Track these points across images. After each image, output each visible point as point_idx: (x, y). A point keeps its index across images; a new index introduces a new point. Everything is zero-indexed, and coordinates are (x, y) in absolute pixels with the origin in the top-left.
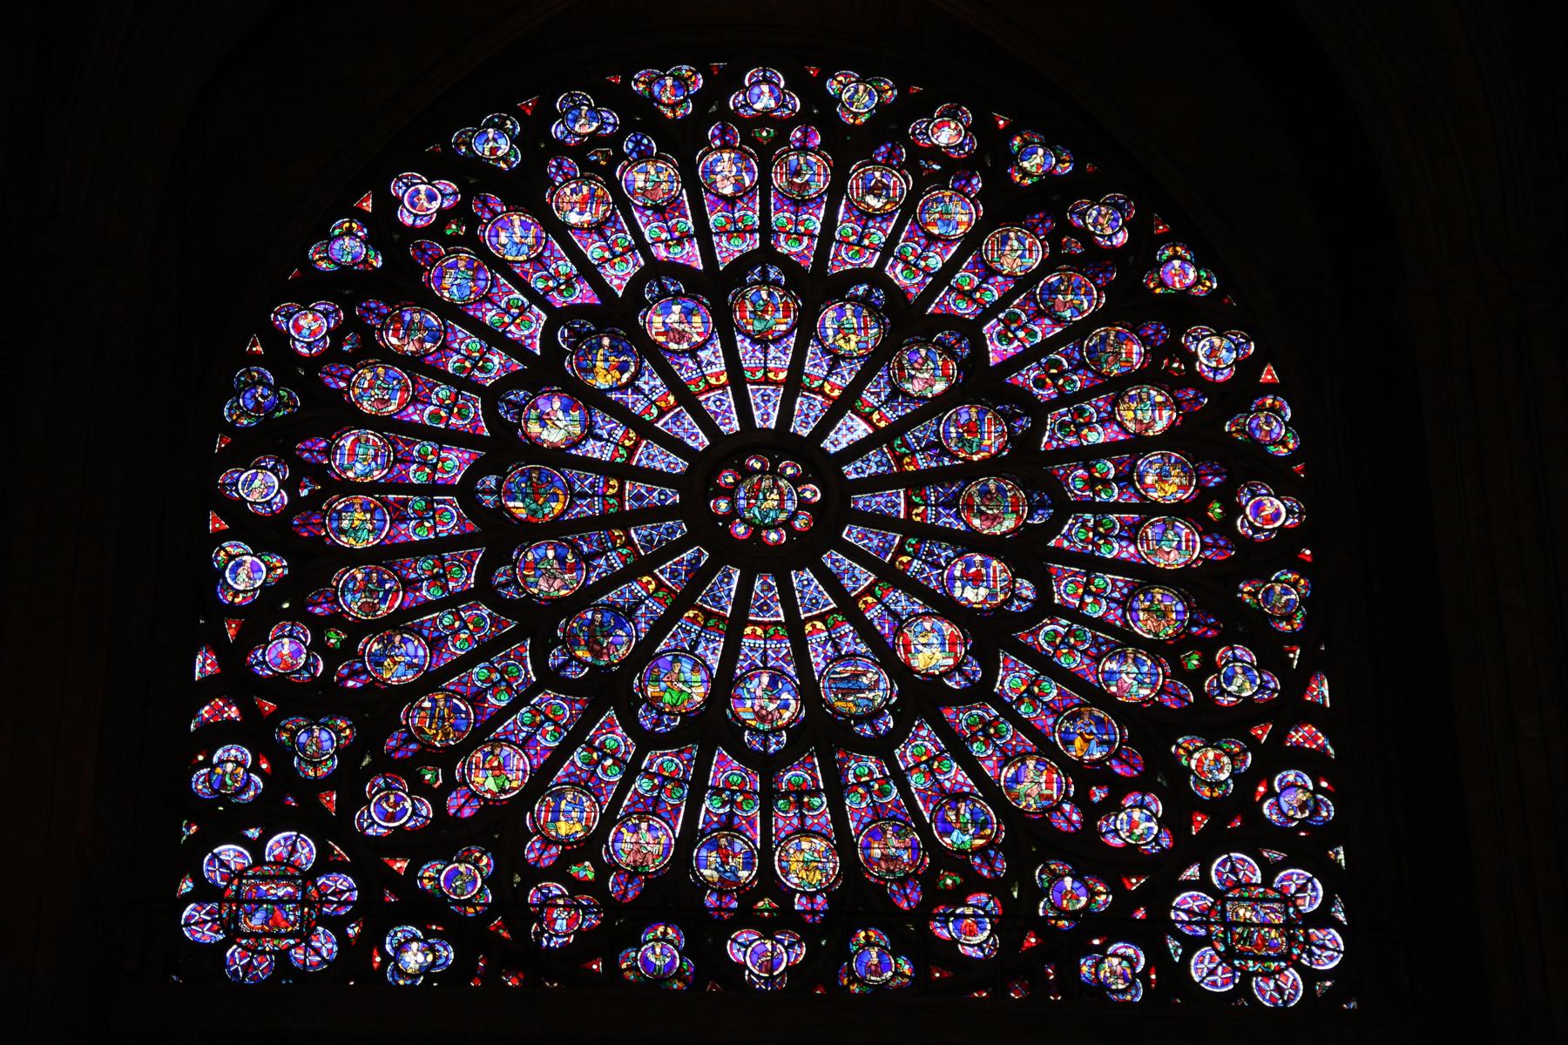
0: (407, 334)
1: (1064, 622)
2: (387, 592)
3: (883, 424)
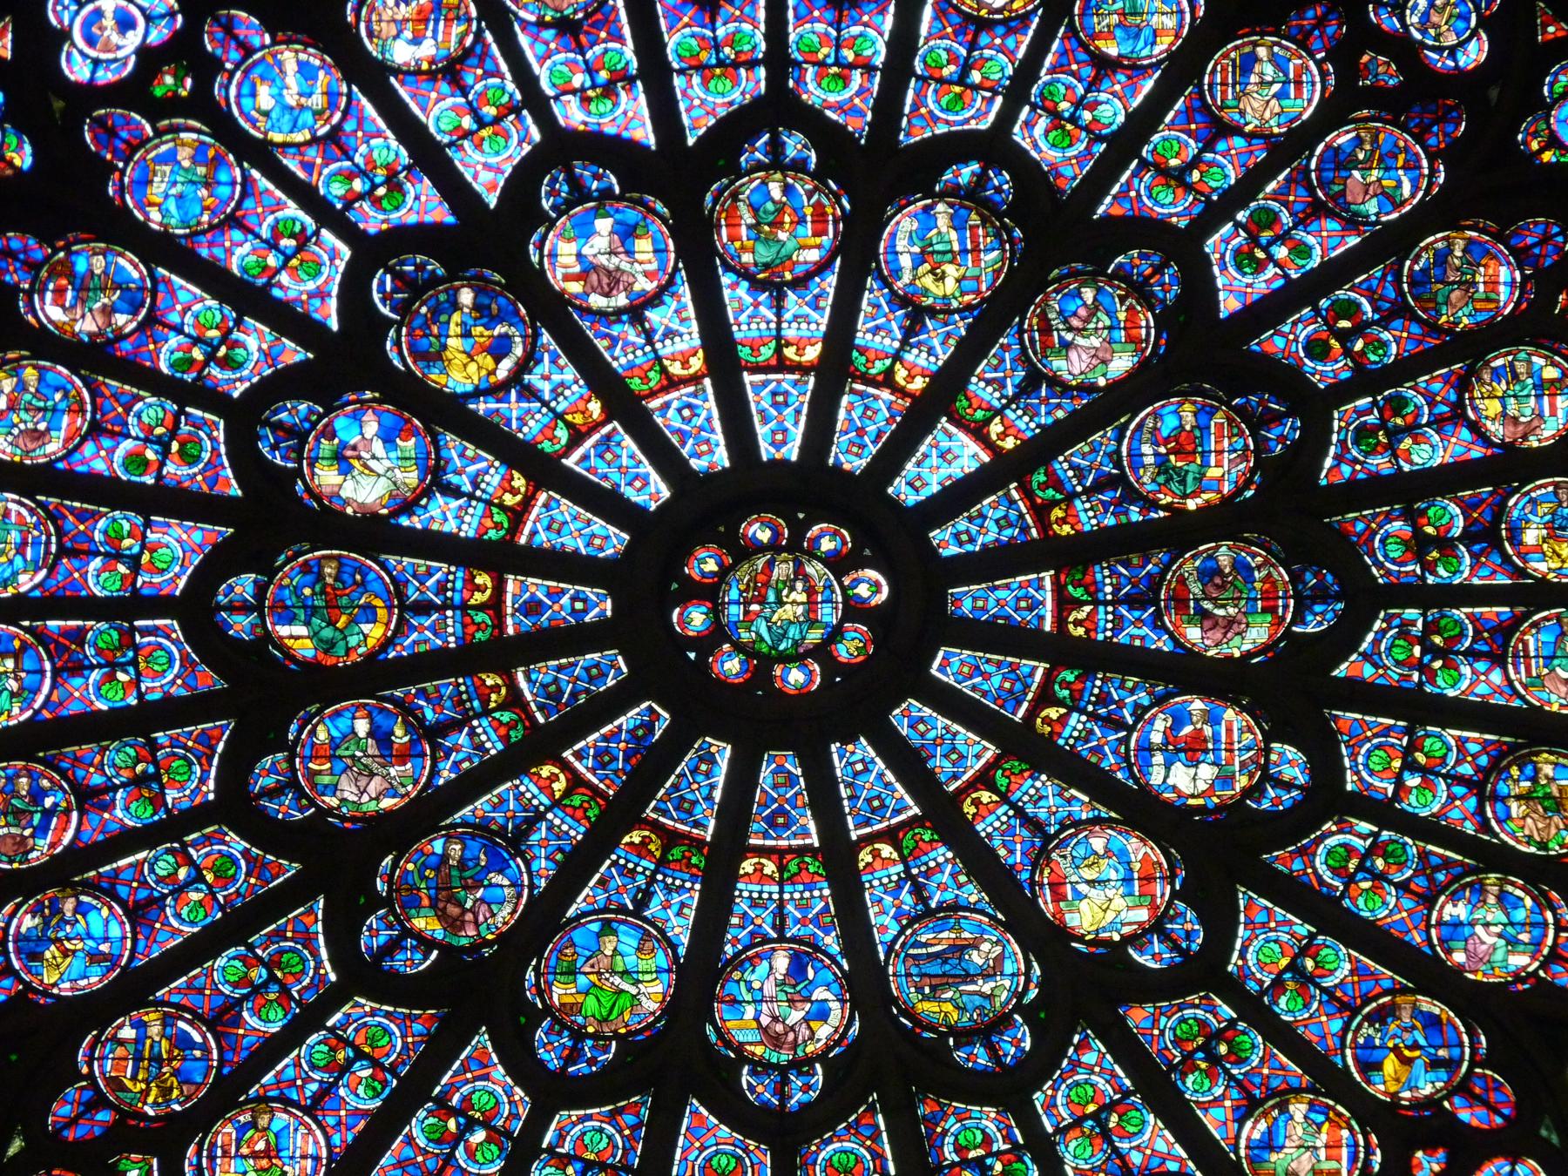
0: (81, 300)
1: (1365, 827)
2: (48, 814)
3: (1009, 443)
